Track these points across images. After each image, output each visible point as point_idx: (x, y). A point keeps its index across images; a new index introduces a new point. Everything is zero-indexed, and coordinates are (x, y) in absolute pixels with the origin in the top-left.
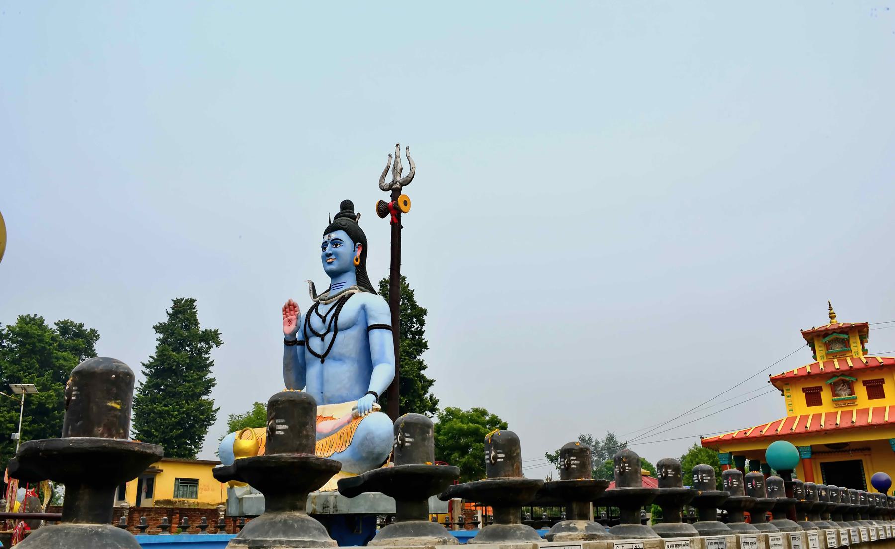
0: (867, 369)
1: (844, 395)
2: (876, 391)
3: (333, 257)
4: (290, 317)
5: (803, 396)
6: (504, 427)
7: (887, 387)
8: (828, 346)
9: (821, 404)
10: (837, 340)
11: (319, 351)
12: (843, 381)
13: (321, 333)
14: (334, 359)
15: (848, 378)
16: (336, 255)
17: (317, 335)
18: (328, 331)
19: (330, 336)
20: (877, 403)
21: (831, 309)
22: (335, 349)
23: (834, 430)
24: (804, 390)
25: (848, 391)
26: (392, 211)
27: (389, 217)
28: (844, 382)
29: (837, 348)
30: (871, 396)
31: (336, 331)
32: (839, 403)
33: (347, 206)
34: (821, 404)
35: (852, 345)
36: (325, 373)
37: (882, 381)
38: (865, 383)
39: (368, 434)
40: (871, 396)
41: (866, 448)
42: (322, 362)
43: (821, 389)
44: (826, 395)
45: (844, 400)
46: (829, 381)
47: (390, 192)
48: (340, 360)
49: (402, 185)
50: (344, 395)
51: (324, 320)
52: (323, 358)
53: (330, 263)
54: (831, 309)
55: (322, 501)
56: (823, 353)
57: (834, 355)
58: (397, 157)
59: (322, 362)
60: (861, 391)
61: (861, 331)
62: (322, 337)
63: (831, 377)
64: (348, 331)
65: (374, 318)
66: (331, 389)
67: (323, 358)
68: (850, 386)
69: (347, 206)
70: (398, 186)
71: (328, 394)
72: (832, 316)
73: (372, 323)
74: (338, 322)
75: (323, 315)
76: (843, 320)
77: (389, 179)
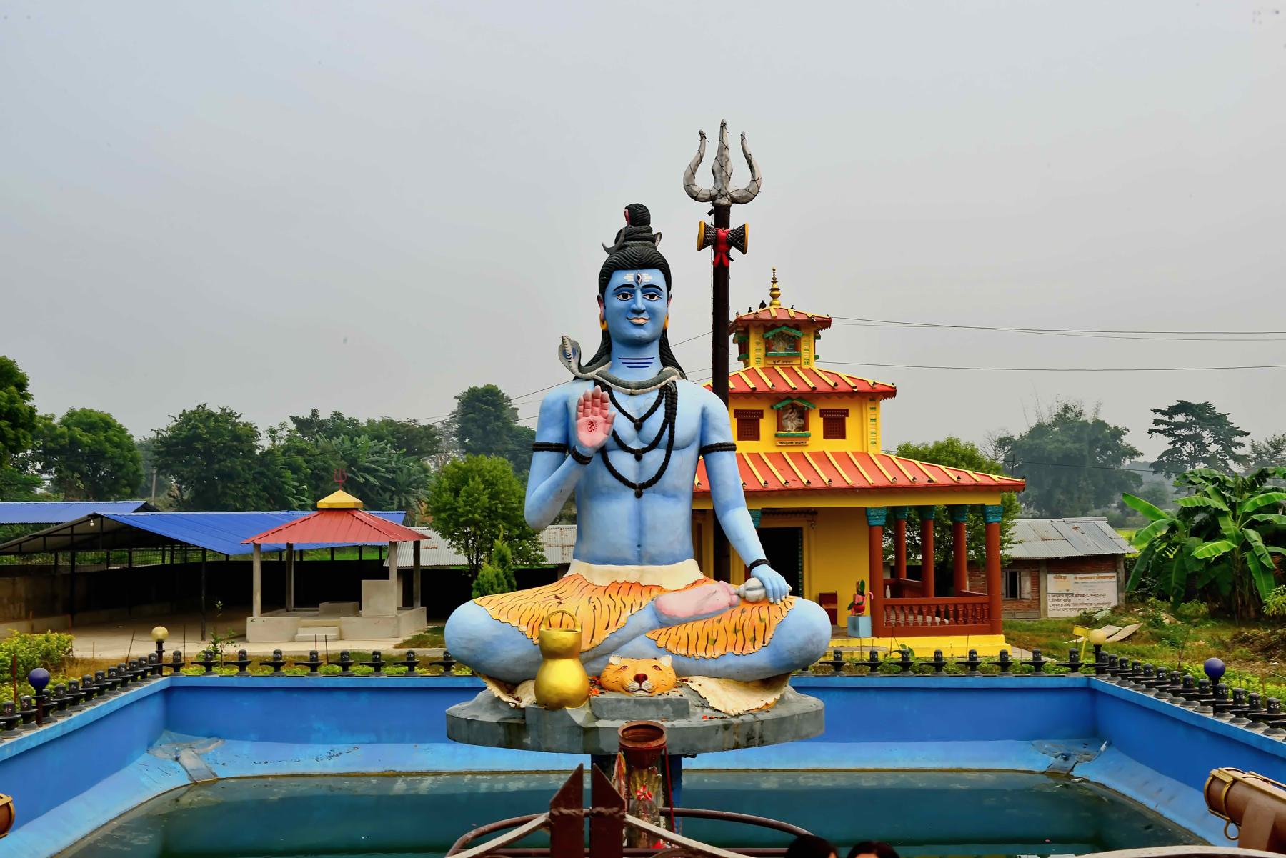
0: (834, 394)
1: (791, 426)
2: (835, 428)
3: (645, 315)
4: (592, 418)
6: (21, 385)
7: (851, 424)
9: (757, 438)
10: (782, 337)
11: (631, 477)
12: (794, 406)
13: (635, 445)
14: (665, 494)
16: (653, 313)
17: (623, 447)
18: (654, 445)
20: (834, 445)
21: (774, 281)
22: (668, 478)
23: (804, 490)
25: (797, 422)
26: (723, 240)
27: (709, 251)
28: (794, 407)
29: (780, 349)
30: (828, 434)
31: (670, 447)
32: (785, 440)
33: (638, 216)
34: (757, 438)
35: (803, 347)
36: (648, 515)
37: (846, 413)
38: (823, 413)
39: (814, 636)
40: (828, 434)
42: (639, 495)
44: (767, 426)
45: (793, 436)
46: (779, 406)
47: (709, 206)
48: (674, 496)
49: (734, 201)
50: (677, 552)
51: (639, 425)
52: (639, 490)
53: (640, 326)
54: (774, 281)
55: (746, 731)
56: (761, 353)
57: (777, 359)
58: (723, 148)
59: (639, 495)
60: (816, 424)
61: (817, 326)
62: (638, 455)
63: (781, 401)
64: (687, 450)
65: (722, 433)
66: (655, 543)
67: (639, 490)
68: (803, 415)
69: (638, 216)
70: (724, 201)
71: (652, 550)
73: (716, 439)
74: (676, 435)
75: (636, 417)
77: (705, 182)
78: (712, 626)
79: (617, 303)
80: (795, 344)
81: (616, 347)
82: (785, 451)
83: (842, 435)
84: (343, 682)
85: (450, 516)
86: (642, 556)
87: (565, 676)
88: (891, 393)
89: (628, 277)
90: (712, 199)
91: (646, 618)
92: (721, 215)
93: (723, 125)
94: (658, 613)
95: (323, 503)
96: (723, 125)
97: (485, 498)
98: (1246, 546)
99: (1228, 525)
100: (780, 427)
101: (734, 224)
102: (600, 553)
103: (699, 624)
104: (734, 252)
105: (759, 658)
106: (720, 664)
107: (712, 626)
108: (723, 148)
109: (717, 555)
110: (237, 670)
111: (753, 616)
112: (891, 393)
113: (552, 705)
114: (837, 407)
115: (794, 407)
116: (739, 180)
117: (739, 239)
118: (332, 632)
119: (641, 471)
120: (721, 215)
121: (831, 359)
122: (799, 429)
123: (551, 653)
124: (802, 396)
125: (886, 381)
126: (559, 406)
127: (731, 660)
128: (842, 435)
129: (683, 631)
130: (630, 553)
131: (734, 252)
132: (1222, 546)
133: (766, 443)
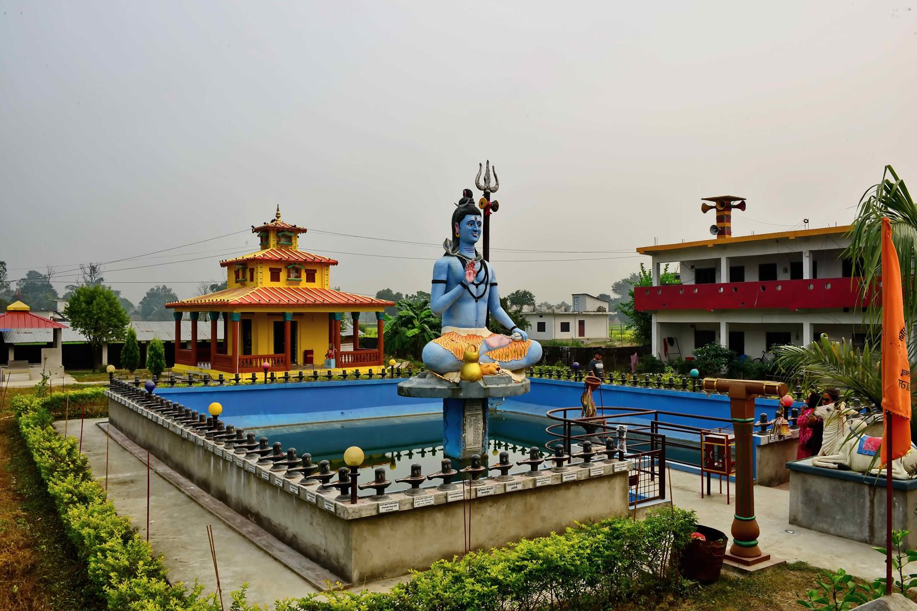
1: (293, 276)
2: (311, 278)
5: (269, 273)
7: (317, 276)
8: (279, 239)
9: (279, 280)
15: (297, 266)
17: (473, 283)
19: (482, 287)
20: (310, 285)
24: (270, 269)
29: (283, 241)
33: (468, 194)
34: (279, 280)
37: (315, 271)
38: (306, 271)
41: (301, 315)
43: (280, 270)
44: (283, 275)
52: (477, 299)
56: (275, 243)
57: (282, 246)
58: (488, 171)
60: (304, 276)
61: (296, 231)
62: (477, 286)
63: (290, 264)
67: (477, 299)
68: (298, 271)
69: (468, 194)
72: (278, 216)
76: (287, 220)
78: (506, 350)
79: (469, 227)
80: (289, 239)
81: (461, 243)
82: (291, 287)
83: (314, 281)
84: (207, 389)
85: (87, 315)
86: (477, 326)
87: (474, 369)
88: (336, 263)
89: (473, 218)
90: (485, 190)
91: (484, 348)
92: (487, 195)
93: (488, 162)
94: (488, 345)
95: (11, 307)
96: (488, 162)
97: (107, 306)
98: (423, 330)
99: (416, 323)
100: (289, 276)
101: (491, 200)
102: (463, 323)
103: (501, 350)
104: (491, 211)
105: (522, 361)
106: (510, 364)
107: (506, 350)
108: (488, 171)
109: (496, 327)
110: (203, 384)
111: (520, 346)
112: (336, 263)
113: (473, 380)
114: (312, 268)
115: (294, 268)
116: (493, 184)
117: (495, 207)
118: (27, 376)
119: (478, 291)
120: (487, 195)
121: (304, 246)
122: (297, 277)
123: (469, 360)
124: (300, 263)
125: (333, 258)
126: (447, 266)
127: (514, 362)
128: (314, 281)
129: (497, 352)
130: (474, 324)
131: (491, 211)
132: (416, 331)
133: (282, 284)
